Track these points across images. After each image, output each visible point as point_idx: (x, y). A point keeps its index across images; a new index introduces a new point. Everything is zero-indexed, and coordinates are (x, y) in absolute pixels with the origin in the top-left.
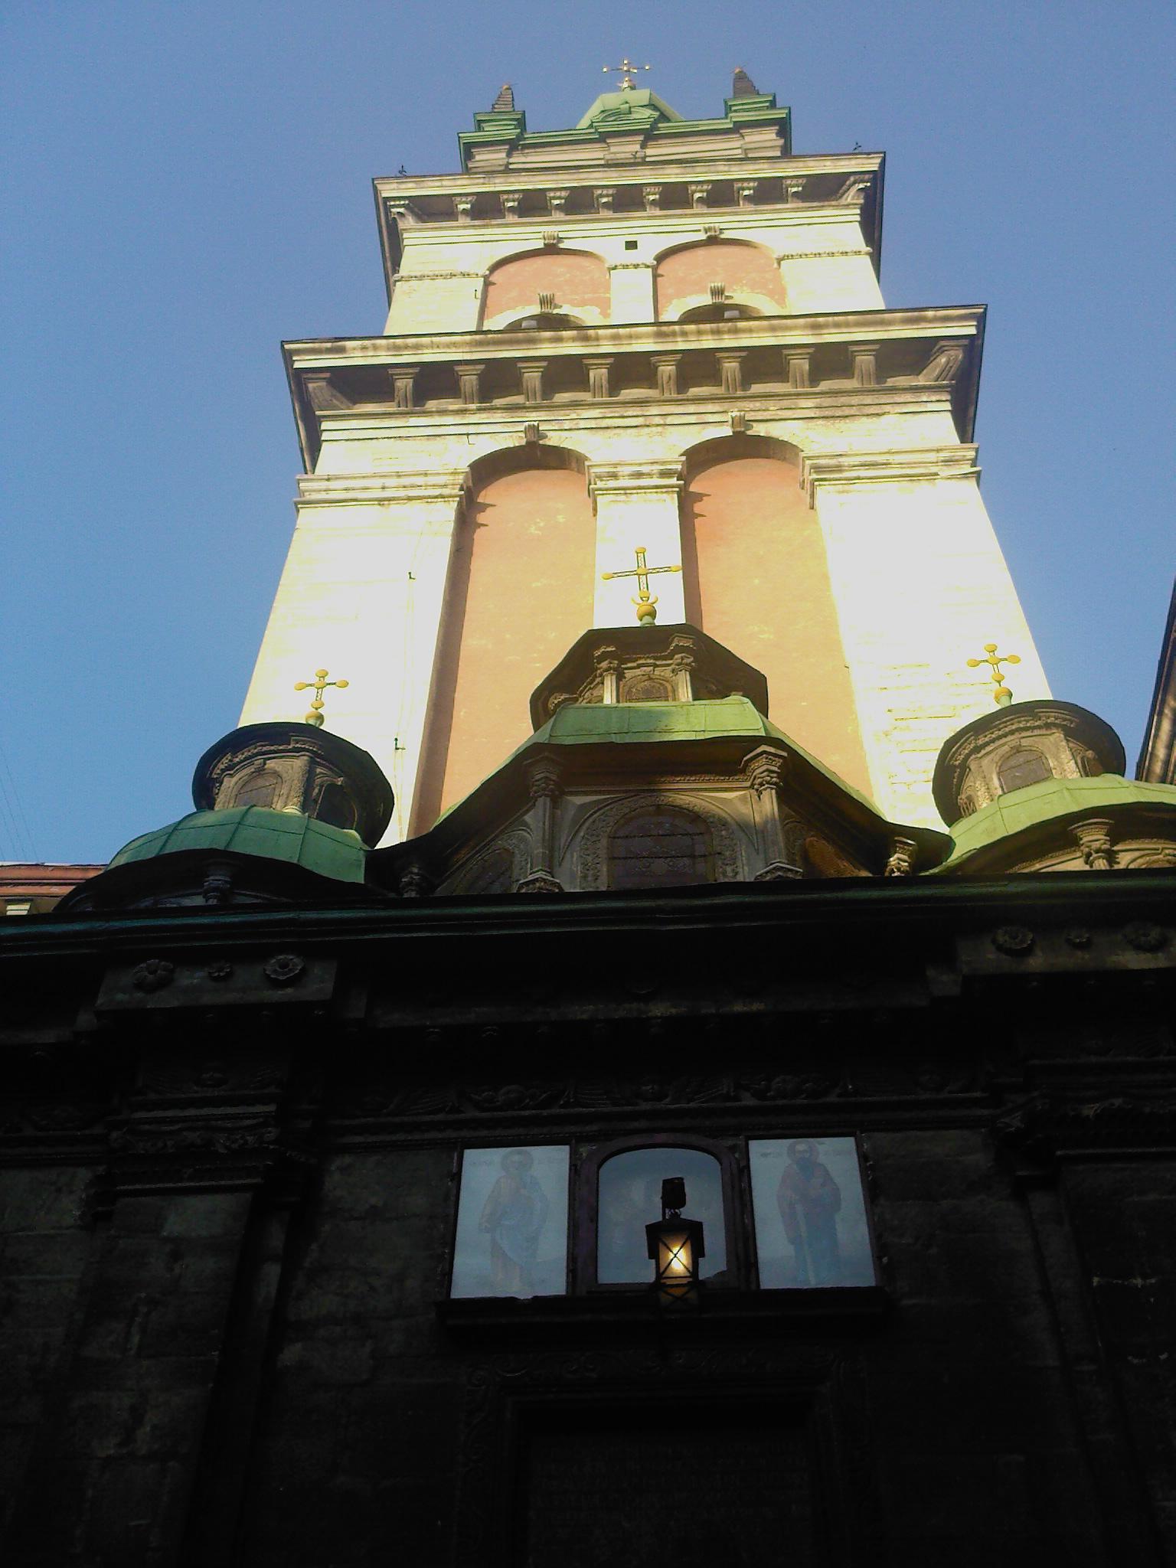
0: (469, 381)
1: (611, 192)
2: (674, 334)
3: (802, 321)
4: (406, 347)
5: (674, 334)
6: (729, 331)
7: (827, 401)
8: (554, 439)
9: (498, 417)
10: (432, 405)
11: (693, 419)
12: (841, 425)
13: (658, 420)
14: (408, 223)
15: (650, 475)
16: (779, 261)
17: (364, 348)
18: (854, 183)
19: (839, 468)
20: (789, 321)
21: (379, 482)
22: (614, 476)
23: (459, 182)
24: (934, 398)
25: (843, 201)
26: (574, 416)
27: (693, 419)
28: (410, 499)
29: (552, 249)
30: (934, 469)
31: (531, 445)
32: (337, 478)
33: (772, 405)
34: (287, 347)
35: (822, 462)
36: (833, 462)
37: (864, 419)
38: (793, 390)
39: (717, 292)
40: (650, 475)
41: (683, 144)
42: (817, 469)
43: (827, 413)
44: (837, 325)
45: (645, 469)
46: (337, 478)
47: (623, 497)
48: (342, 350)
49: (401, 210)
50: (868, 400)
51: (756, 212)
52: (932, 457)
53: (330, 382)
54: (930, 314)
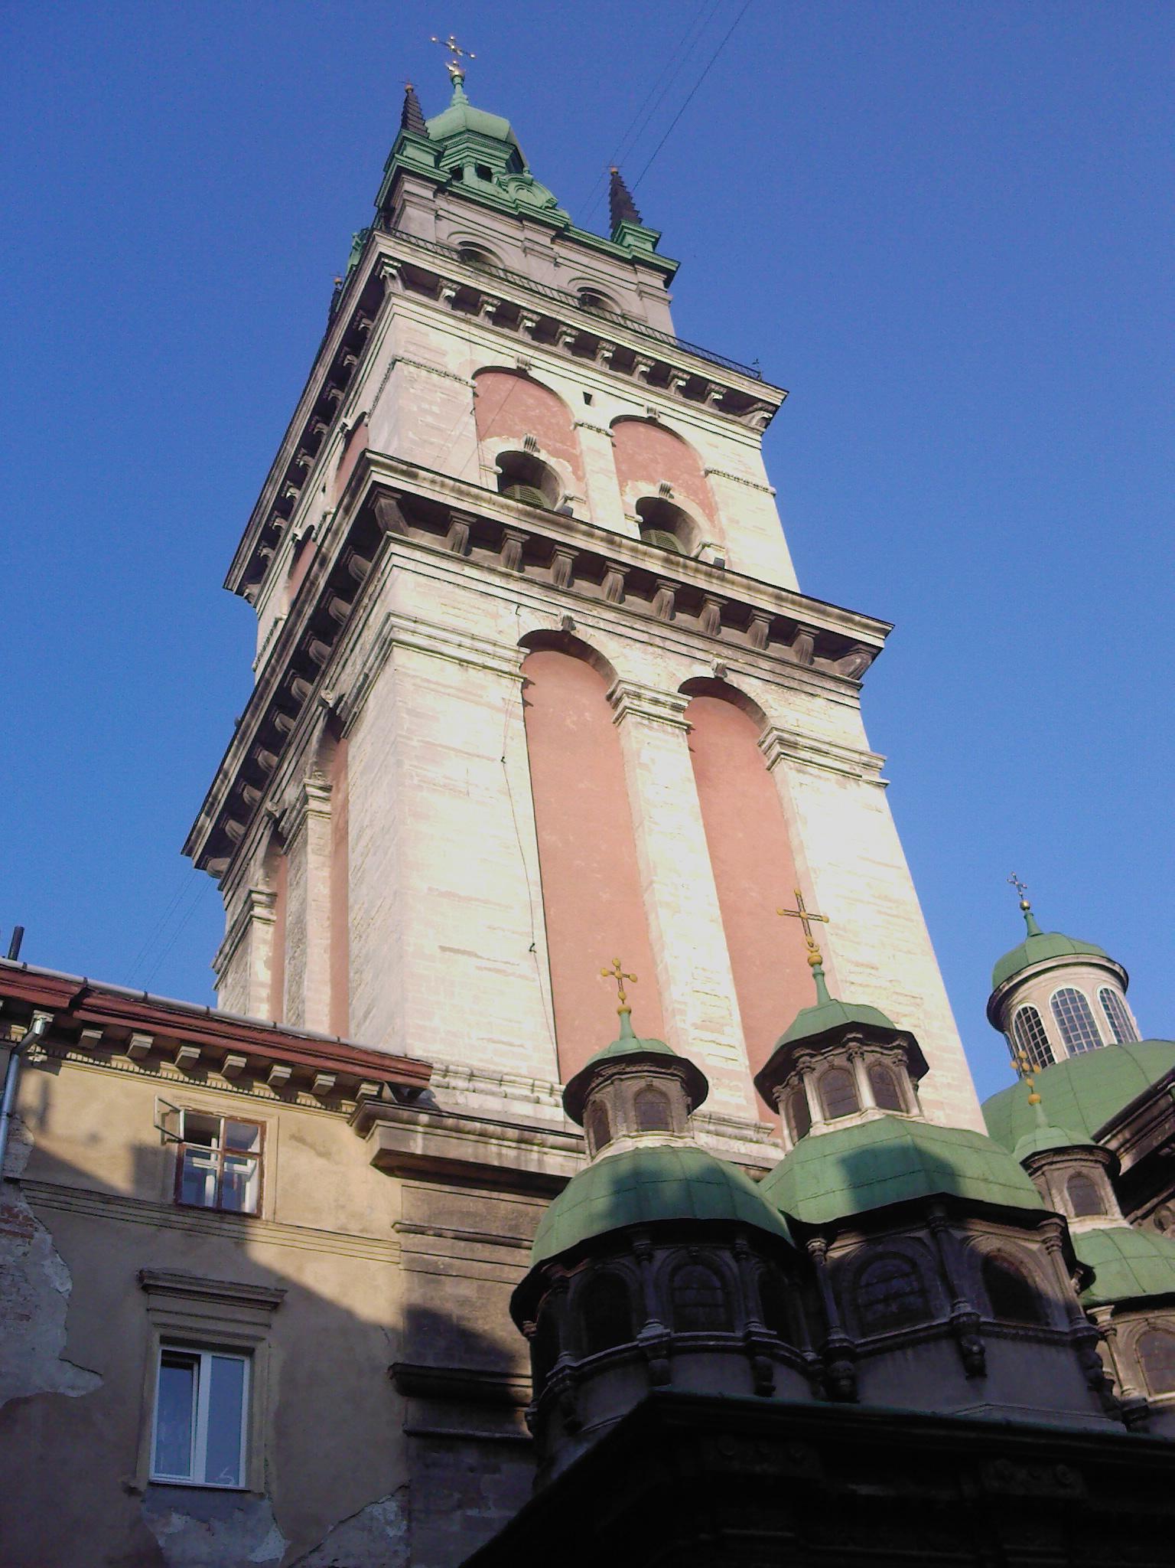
1: (574, 333)
2: (678, 564)
3: (771, 589)
4: (468, 494)
5: (678, 564)
6: (718, 578)
7: (778, 668)
8: (582, 633)
9: (535, 591)
10: (478, 553)
11: (684, 650)
12: (788, 694)
13: (658, 641)
14: (396, 287)
15: (664, 704)
16: (707, 472)
17: (433, 482)
18: (761, 409)
19: (794, 746)
21: (457, 639)
22: (638, 696)
23: (449, 266)
24: (849, 693)
25: (744, 420)
26: (595, 613)
27: (684, 650)
28: (485, 667)
29: (521, 373)
31: (565, 633)
33: (738, 655)
34: (368, 455)
35: (786, 736)
36: (792, 738)
37: (803, 696)
38: (750, 647)
39: (665, 489)
40: (664, 704)
41: (586, 255)
42: (782, 741)
43: (778, 680)
44: (793, 602)
45: (662, 698)
47: (646, 722)
48: (415, 476)
49: (394, 272)
50: (806, 677)
51: (685, 405)
53: (399, 503)
54: (857, 618)
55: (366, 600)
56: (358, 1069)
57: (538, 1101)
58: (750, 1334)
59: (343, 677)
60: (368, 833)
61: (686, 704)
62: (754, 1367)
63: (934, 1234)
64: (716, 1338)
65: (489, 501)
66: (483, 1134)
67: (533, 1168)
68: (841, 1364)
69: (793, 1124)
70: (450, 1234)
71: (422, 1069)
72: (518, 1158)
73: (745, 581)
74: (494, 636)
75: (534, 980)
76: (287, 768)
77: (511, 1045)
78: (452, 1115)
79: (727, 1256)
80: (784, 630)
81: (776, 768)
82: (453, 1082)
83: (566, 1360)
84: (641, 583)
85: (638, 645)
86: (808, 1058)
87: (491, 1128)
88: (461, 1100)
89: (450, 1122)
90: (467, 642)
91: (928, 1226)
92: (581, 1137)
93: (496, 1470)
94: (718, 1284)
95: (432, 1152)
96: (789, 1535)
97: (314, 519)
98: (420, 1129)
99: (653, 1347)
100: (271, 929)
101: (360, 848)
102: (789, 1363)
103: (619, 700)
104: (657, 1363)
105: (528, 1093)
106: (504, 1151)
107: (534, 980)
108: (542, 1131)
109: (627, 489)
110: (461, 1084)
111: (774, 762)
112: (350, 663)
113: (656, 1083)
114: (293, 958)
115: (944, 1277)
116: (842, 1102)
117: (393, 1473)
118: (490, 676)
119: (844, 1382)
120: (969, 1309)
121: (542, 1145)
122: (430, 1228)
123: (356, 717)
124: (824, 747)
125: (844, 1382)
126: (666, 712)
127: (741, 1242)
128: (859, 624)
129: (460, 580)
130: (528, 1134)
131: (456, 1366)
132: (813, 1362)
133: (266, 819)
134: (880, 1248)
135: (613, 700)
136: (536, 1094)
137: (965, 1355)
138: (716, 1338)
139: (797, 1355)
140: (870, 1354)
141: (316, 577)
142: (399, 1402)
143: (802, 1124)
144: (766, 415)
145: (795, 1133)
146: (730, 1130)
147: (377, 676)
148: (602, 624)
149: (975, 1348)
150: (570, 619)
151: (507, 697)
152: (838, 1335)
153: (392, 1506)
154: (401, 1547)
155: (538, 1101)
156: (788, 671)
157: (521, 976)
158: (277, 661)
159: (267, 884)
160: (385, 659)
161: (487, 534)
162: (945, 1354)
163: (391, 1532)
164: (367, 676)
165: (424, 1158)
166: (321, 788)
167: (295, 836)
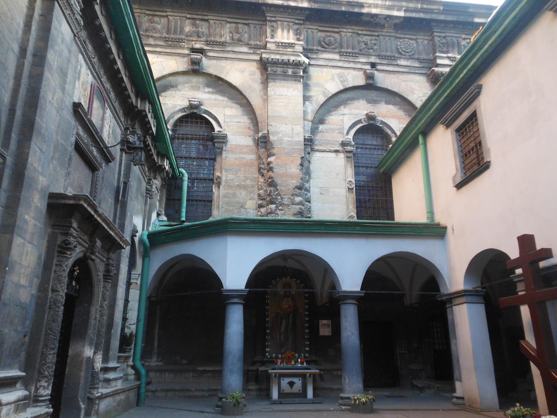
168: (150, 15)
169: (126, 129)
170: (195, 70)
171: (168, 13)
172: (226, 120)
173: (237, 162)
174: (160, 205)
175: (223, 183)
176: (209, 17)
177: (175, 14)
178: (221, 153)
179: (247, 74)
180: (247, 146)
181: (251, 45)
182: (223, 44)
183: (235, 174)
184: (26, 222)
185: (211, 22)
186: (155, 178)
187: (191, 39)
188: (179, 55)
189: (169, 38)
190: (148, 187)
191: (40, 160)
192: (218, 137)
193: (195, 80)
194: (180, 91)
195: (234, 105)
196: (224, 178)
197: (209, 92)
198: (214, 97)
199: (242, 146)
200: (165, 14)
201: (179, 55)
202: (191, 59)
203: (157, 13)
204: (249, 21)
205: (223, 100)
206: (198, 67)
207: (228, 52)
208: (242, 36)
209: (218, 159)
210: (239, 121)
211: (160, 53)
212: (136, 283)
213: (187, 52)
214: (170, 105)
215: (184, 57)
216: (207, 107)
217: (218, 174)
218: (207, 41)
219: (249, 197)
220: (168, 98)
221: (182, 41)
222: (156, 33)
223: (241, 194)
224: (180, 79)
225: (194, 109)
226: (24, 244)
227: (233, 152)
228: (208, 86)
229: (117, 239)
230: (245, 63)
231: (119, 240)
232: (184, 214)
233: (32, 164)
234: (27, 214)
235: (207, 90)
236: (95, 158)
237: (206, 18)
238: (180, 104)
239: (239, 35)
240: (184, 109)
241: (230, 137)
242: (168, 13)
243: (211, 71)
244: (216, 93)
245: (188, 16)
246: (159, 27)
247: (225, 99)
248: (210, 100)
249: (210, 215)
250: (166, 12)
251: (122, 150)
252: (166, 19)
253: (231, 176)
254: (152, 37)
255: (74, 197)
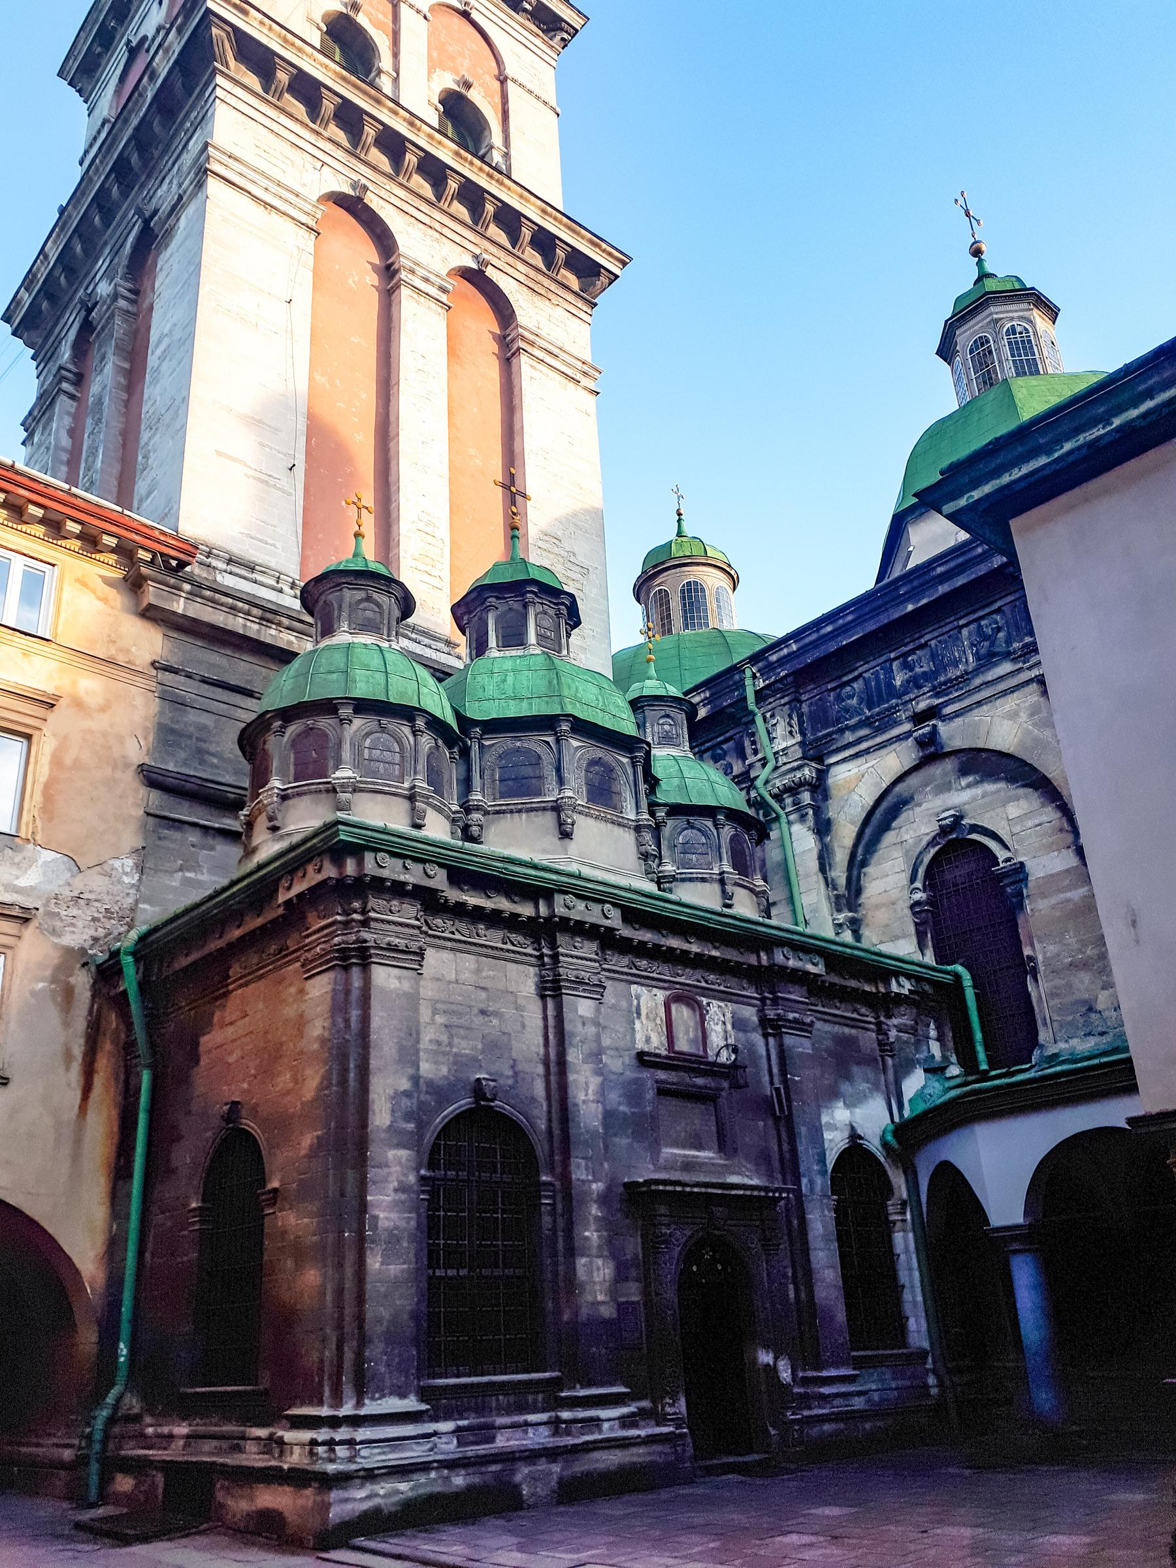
0: (328, 106)
3: (539, 203)
4: (293, 44)
5: (466, 160)
6: (498, 181)
7: (532, 274)
11: (458, 239)
12: (537, 299)
13: (437, 226)
15: (433, 284)
17: (262, 23)
20: (533, 198)
22: (413, 272)
24: (585, 308)
26: (388, 187)
27: (458, 239)
30: (579, 376)
32: (236, 159)
33: (502, 254)
36: (532, 337)
42: (524, 338)
43: (530, 285)
44: (555, 219)
45: (432, 278)
46: (236, 159)
47: (415, 296)
48: (246, 13)
52: (579, 365)
54: (604, 246)
55: (188, 124)
56: (137, 538)
57: (281, 591)
58: (414, 787)
59: (159, 193)
60: (166, 342)
61: (450, 287)
62: (413, 809)
63: (558, 741)
64: (389, 786)
65: (310, 56)
66: (233, 608)
67: (269, 641)
68: (476, 816)
69: (474, 645)
70: (198, 677)
71: (190, 548)
72: (259, 631)
73: (519, 190)
74: (296, 187)
75: (290, 495)
76: (102, 264)
77: (266, 543)
78: (210, 589)
79: (407, 730)
80: (544, 242)
81: (514, 361)
82: (215, 563)
83: (276, 783)
84: (433, 170)
85: (421, 225)
86: (493, 600)
87: (240, 604)
88: (219, 578)
89: (208, 593)
90: (273, 188)
91: (556, 734)
92: (311, 625)
93: (212, 848)
94: (397, 750)
95: (190, 614)
96: (417, 923)
97: (148, 29)
98: (183, 594)
99: (342, 786)
100: (75, 404)
101: (159, 352)
102: (439, 810)
103: (397, 271)
104: (343, 796)
105: (272, 582)
106: (249, 624)
107: (290, 495)
108: (283, 615)
109: (434, 76)
110: (221, 565)
111: (513, 354)
112: (167, 180)
113: (375, 596)
114: (92, 433)
115: (558, 770)
116: (513, 637)
117: (131, 839)
118: (290, 225)
119: (474, 828)
120: (570, 794)
121: (279, 624)
122: (183, 670)
123: (169, 233)
124: (556, 351)
125: (474, 828)
126: (434, 291)
127: (420, 723)
128: (604, 251)
129: (275, 127)
130: (269, 614)
131: (192, 773)
132: (457, 812)
133: (79, 306)
134: (518, 744)
135: (389, 273)
136: (280, 585)
137: (561, 824)
138: (389, 786)
139: (445, 805)
140: (498, 812)
141: (145, 89)
142: (143, 791)
143: (479, 648)
144: (566, 36)
145: (474, 652)
146: (427, 641)
147: (191, 199)
148: (393, 200)
149: (569, 820)
150: (365, 188)
151: (301, 246)
152: (476, 797)
153: (129, 863)
154: (132, 891)
155: (281, 591)
156: (540, 278)
157: (279, 489)
158: (101, 162)
159: (75, 364)
160: (200, 185)
161: (307, 90)
162: (549, 818)
163: (126, 880)
164: (180, 197)
165: (184, 616)
166: (129, 290)
167: (103, 329)
168: (834, 689)
169: (763, 1000)
170: (931, 752)
171: (861, 670)
172: (1015, 830)
173: (1058, 914)
174: (943, 1046)
175: (1042, 968)
176: (927, 637)
177: (874, 663)
178: (1021, 906)
179: (1023, 716)
180: (1067, 871)
181: (1015, 652)
182: (966, 677)
183: (1060, 942)
184: (587, 1238)
185: (933, 643)
186: (890, 1017)
187: (907, 698)
188: (898, 738)
189: (872, 716)
190: (880, 1037)
191: (586, 1165)
192: (1006, 874)
193: (938, 770)
194: (920, 805)
195: (1022, 791)
196: (1040, 958)
197: (969, 786)
198: (978, 791)
199: (1058, 874)
200: (856, 673)
201: (898, 738)
202: (916, 739)
203: (845, 679)
204: (998, 604)
205: (999, 791)
206: (932, 749)
207: (978, 689)
208: (992, 644)
209: (1021, 920)
210: (1037, 822)
211: (867, 751)
212: (904, 1221)
213: (907, 727)
214: (911, 841)
215: (907, 738)
216: (973, 817)
217: (1027, 951)
218: (934, 688)
219: (1099, 986)
220: (903, 829)
221: (893, 709)
222: (851, 717)
223: (1082, 982)
224: (913, 781)
225: (950, 833)
226: (591, 1262)
227: (1043, 896)
228: (963, 771)
229: (756, 1193)
230: (1015, 694)
231: (763, 1194)
232: (982, 1055)
233: (578, 1179)
234: (586, 1230)
235: (964, 782)
236: (706, 1087)
237: (923, 641)
238: (928, 831)
239: (986, 644)
240: (934, 838)
241: (1030, 866)
242: (861, 670)
243: (958, 744)
244: (981, 781)
245: (892, 655)
246: (854, 702)
247: (1001, 785)
248: (974, 799)
249: (1033, 1041)
250: (857, 669)
251: (765, 1036)
252: (861, 681)
253: (1052, 949)
254: (848, 728)
255: (648, 1183)
